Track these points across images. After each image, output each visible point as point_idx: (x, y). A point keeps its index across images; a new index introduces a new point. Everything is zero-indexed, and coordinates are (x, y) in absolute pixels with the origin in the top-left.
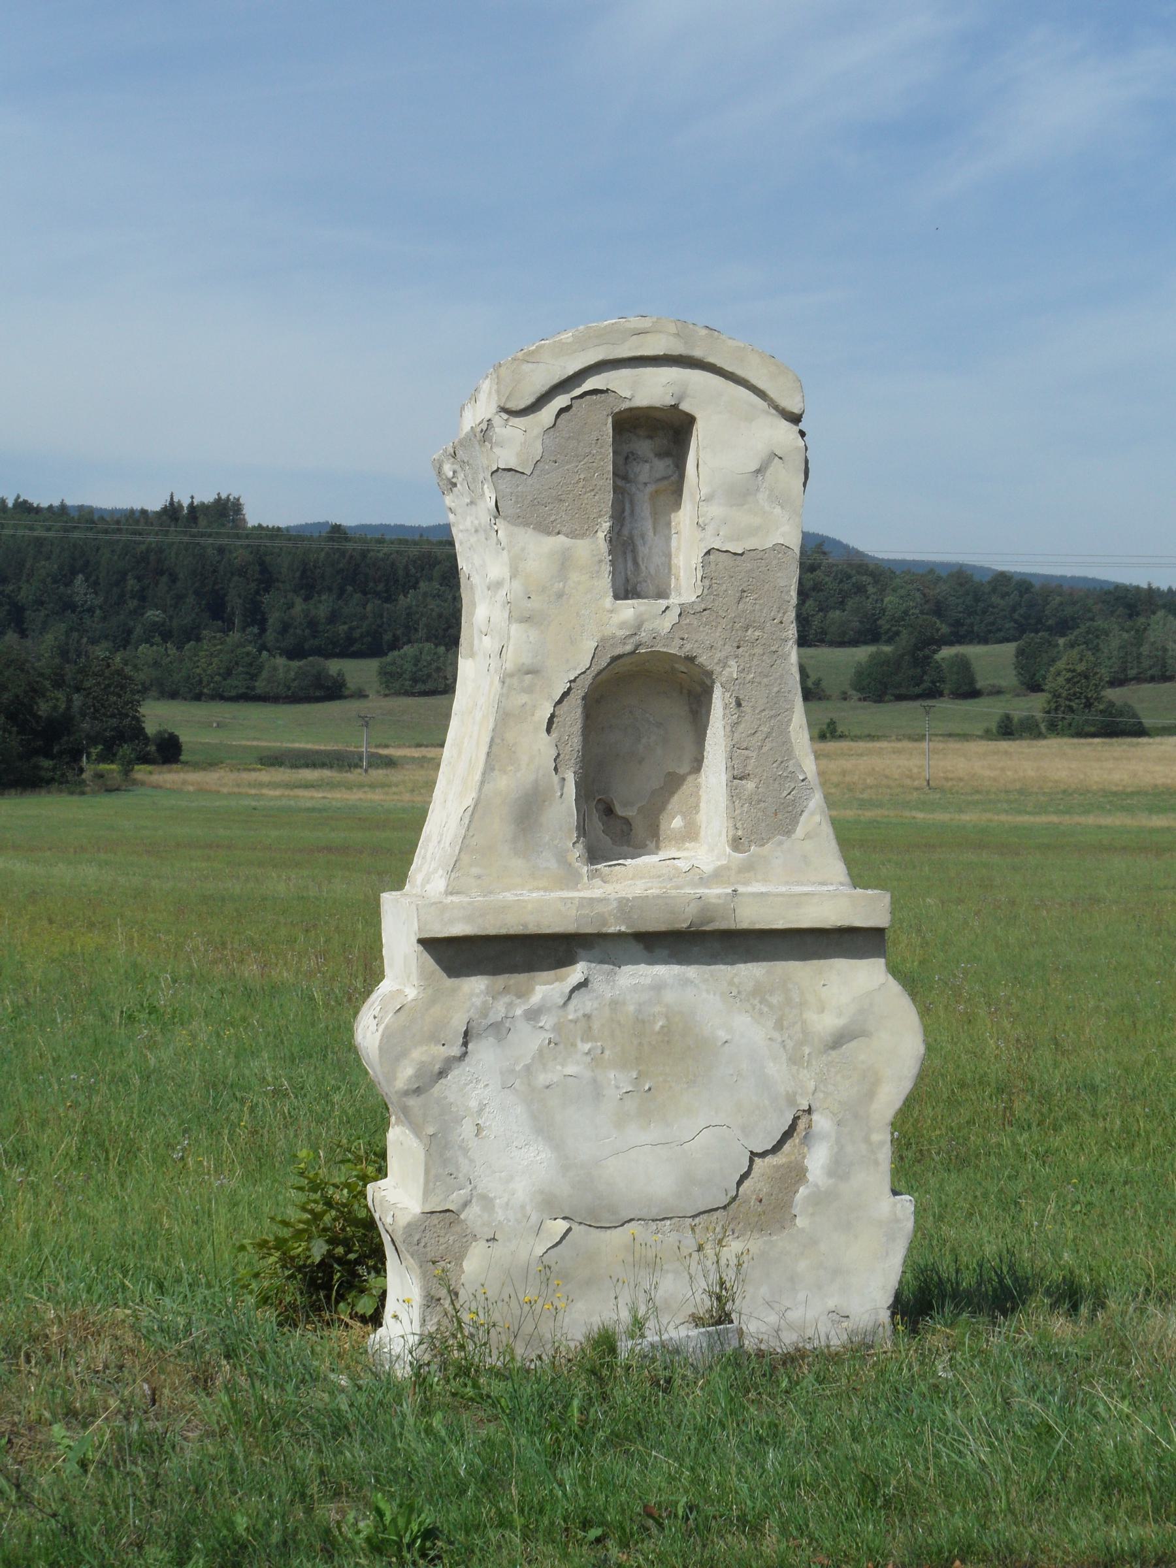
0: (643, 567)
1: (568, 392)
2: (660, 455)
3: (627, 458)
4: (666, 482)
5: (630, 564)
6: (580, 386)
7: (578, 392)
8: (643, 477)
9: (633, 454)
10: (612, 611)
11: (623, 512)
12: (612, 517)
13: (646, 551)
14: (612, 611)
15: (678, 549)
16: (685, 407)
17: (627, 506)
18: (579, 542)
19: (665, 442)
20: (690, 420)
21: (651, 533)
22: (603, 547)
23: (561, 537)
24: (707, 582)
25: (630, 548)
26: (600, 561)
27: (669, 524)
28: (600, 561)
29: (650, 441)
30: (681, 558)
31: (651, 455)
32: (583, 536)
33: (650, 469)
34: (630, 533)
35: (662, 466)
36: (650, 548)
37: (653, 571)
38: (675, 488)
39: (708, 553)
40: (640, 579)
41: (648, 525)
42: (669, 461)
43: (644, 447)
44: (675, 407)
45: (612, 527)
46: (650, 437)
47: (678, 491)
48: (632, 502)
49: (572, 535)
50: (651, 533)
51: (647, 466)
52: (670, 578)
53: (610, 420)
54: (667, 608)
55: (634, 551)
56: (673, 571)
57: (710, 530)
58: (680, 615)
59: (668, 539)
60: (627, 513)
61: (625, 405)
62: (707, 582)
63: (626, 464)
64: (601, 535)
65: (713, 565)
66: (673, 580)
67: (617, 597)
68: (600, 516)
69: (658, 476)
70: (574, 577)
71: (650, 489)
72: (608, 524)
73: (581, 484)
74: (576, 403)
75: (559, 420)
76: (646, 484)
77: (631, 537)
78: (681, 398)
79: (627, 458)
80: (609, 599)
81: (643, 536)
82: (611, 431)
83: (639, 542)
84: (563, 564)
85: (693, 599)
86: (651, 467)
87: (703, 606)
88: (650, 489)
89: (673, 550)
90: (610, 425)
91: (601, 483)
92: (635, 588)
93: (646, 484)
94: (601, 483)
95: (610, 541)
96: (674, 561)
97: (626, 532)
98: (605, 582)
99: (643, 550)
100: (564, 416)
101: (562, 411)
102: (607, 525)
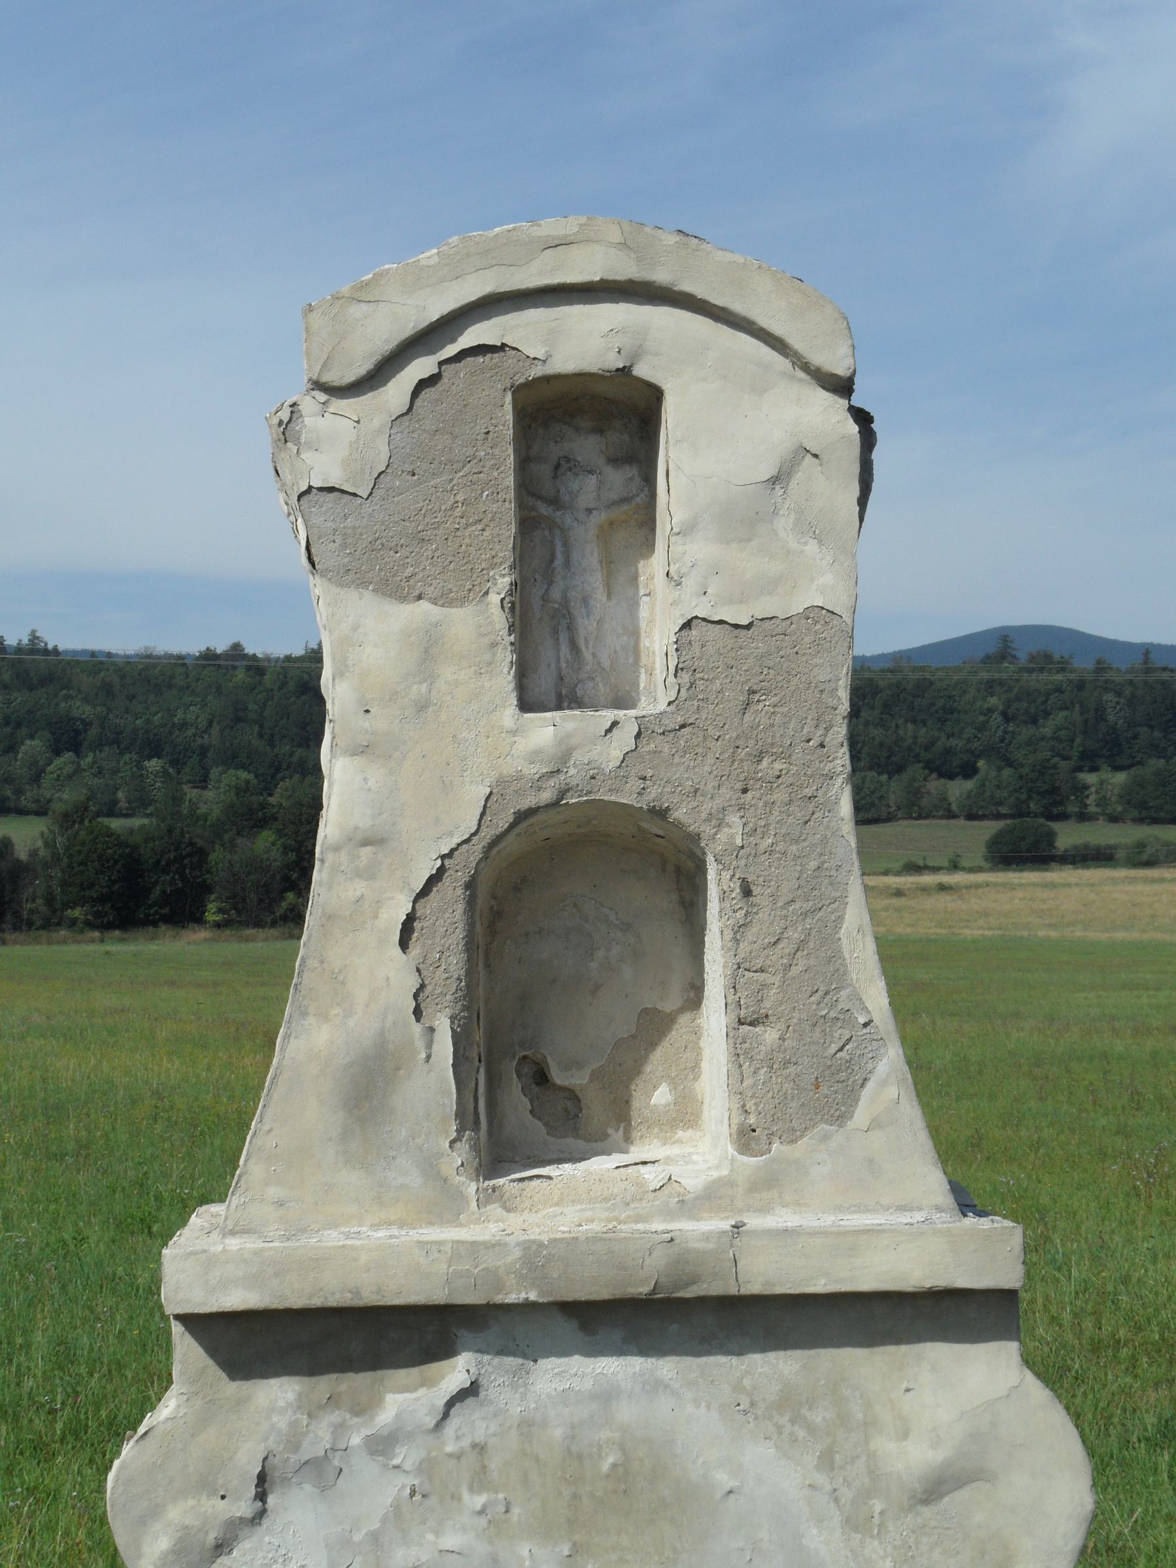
0: (587, 654)
1: (433, 352)
2: (615, 461)
3: (557, 467)
4: (626, 507)
5: (565, 650)
6: (453, 340)
7: (451, 350)
8: (584, 501)
10: (514, 732)
11: (552, 561)
12: (513, 567)
14: (514, 732)
15: (651, 621)
16: (642, 370)
17: (559, 549)
18: (456, 613)
19: (626, 437)
20: (655, 395)
21: (600, 595)
22: (499, 620)
23: (424, 605)
24: (685, 678)
25: (564, 623)
26: (494, 645)
27: (634, 579)
28: (494, 645)
30: (657, 637)
31: (601, 461)
32: (462, 601)
33: (594, 488)
35: (618, 479)
37: (606, 663)
39: (687, 625)
40: (583, 676)
41: (596, 581)
42: (631, 471)
43: (587, 447)
44: (625, 371)
46: (600, 431)
47: (648, 522)
48: (566, 544)
49: (444, 599)
50: (600, 595)
51: (592, 480)
53: (509, 398)
54: (615, 724)
55: (571, 628)
58: (638, 736)
60: (559, 562)
61: (537, 371)
62: (685, 678)
63: (555, 477)
64: (494, 599)
66: (643, 677)
67: (526, 705)
68: (493, 566)
69: (614, 496)
70: (448, 673)
72: (507, 580)
74: (448, 370)
75: (418, 402)
76: (589, 511)
77: (565, 603)
78: (636, 356)
79: (557, 467)
80: (509, 713)
81: (585, 601)
82: (510, 417)
84: (426, 652)
86: (601, 483)
87: (680, 720)
89: (643, 625)
90: (508, 407)
91: (494, 507)
93: (589, 511)
94: (494, 507)
95: (512, 609)
96: (645, 642)
97: (556, 593)
98: (504, 681)
99: (586, 626)
100: (427, 394)
102: (504, 582)
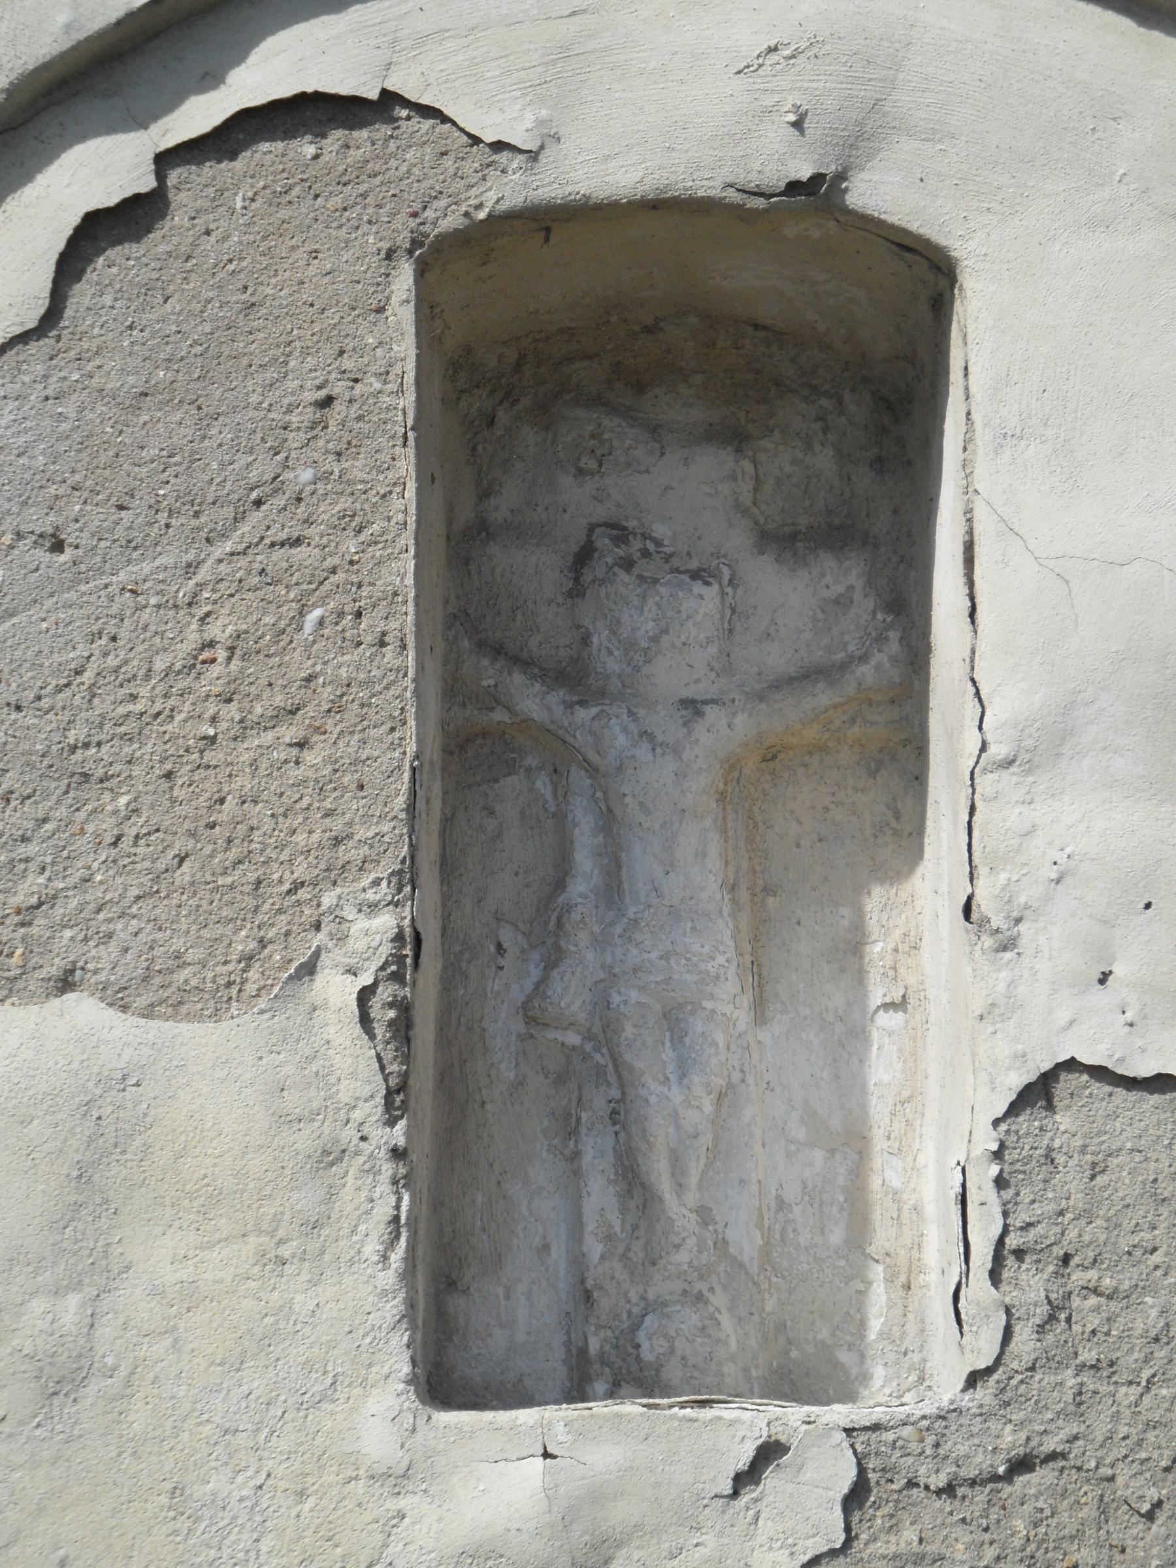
0: (678, 1210)
1: (142, 123)
2: (786, 541)
3: (584, 555)
4: (823, 697)
5: (600, 1195)
6: (211, 79)
7: (200, 115)
8: (675, 672)
9: (620, 533)
10: (398, 1479)
11: (560, 885)
12: (407, 877)
13: (699, 1112)
14: (398, 1479)
15: (907, 1100)
16: (881, 192)
18: (196, 1039)
19: (824, 460)
20: (927, 276)
21: (729, 1000)
22: (353, 1067)
23: (82, 1010)
24: (1031, 1285)
25: (599, 1100)
26: (331, 1157)
27: (852, 948)
28: (331, 1157)
29: (726, 456)
30: (928, 1155)
31: (736, 540)
32: (223, 997)
33: (710, 627)
34: (602, 1005)
35: (795, 602)
36: (726, 1097)
37: (746, 1242)
38: (875, 737)
39: (1038, 1093)
40: (660, 1288)
41: (712, 954)
42: (842, 575)
43: (688, 491)
44: (817, 193)
45: (411, 942)
46: (736, 438)
47: (899, 749)
48: (609, 822)
49: (154, 991)
50: (729, 1000)
51: (704, 603)
52: (857, 1276)
53: (404, 279)
54: (769, 1453)
55: (621, 1116)
56: (882, 1238)
57: (1050, 945)
58: (856, 1497)
59: (849, 1039)
60: (582, 885)
61: (507, 190)
62: (1031, 1285)
63: (577, 591)
64: (336, 990)
65: (1071, 1181)
66: (879, 1297)
67: (444, 1380)
68: (335, 874)
69: (778, 658)
70: (159, 1256)
71: (725, 732)
72: (386, 922)
73: (214, 678)
74: (191, 186)
75: (81, 295)
76: (693, 707)
77: (604, 1030)
78: (860, 140)
79: (584, 555)
80: (381, 1409)
81: (674, 1021)
82: (406, 348)
83: (649, 1059)
84: (82, 1176)
85: (947, 1389)
86: (733, 617)
87: (1011, 1440)
88: (725, 732)
89: (879, 1110)
90: (403, 315)
91: (344, 665)
92: (627, 1341)
93: (693, 707)
94: (344, 665)
95: (403, 1028)
96: (886, 1173)
97: (570, 995)
98: (363, 1292)
99: (675, 1109)
100: (114, 265)
101: (99, 231)
102: (373, 932)
